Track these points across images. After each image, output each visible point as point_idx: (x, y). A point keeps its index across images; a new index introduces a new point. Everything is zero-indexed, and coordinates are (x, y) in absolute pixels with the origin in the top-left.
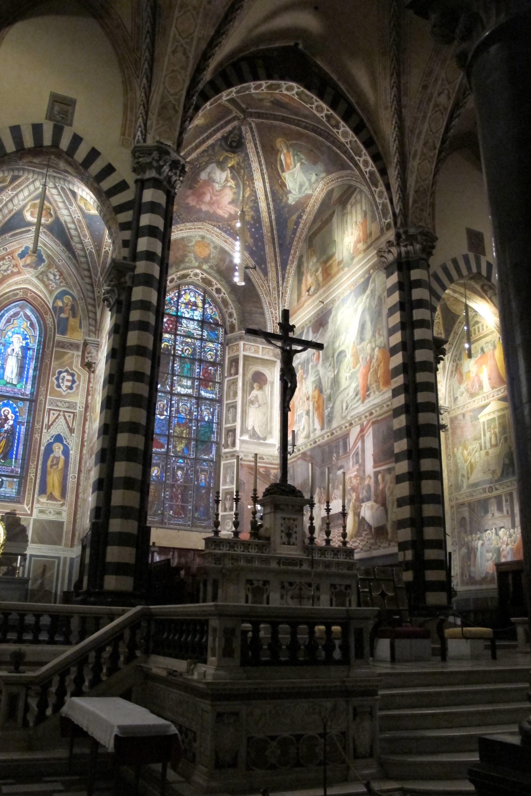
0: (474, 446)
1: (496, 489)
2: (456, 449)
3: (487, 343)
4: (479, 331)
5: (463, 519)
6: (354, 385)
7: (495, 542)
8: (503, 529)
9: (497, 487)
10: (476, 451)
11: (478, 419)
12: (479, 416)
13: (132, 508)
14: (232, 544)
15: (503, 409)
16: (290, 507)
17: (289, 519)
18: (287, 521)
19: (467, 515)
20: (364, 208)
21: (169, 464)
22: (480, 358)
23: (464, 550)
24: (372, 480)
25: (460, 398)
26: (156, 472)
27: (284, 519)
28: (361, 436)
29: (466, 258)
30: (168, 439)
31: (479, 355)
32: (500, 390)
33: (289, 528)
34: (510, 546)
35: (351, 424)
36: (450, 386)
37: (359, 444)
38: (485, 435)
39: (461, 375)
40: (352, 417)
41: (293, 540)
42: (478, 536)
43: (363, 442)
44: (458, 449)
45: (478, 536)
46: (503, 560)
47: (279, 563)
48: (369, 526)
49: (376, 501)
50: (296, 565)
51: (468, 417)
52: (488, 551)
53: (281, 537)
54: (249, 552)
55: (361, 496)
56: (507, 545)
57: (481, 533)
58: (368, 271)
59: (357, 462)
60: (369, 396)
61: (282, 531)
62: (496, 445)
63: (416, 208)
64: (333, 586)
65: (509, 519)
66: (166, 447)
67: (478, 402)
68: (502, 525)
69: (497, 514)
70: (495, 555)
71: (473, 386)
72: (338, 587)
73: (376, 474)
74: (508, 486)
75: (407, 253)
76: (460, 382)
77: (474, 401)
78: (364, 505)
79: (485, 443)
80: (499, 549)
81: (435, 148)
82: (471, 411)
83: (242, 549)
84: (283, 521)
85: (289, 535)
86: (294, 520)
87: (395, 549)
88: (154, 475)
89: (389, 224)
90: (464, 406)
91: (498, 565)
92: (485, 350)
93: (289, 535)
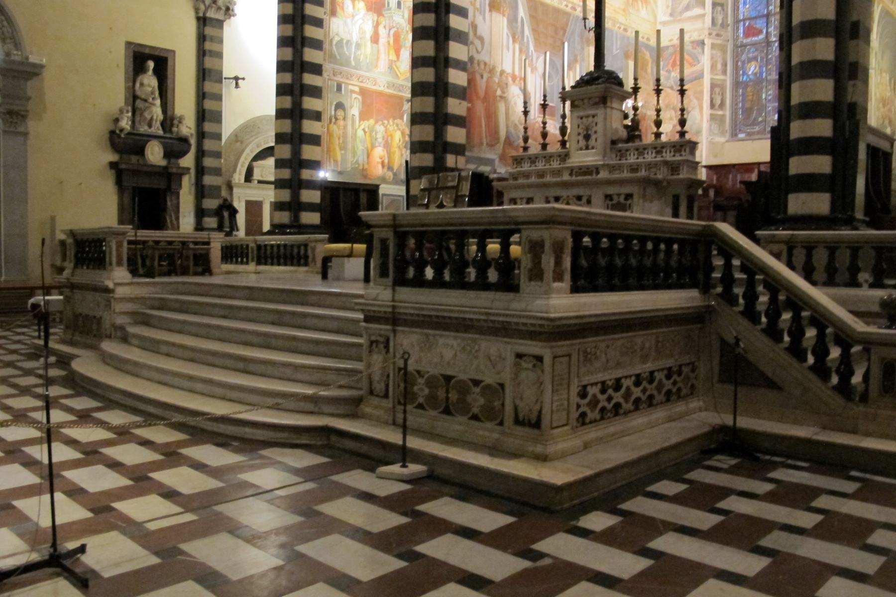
13: (427, 143)
14: (533, 159)
16: (586, 101)
17: (588, 117)
18: (584, 120)
21: (771, 53)
26: (752, 69)
27: (582, 118)
30: (767, 19)
33: (587, 129)
41: (592, 142)
47: (571, 174)
50: (590, 174)
53: (578, 142)
54: (550, 165)
61: (579, 134)
64: (609, 197)
66: (765, 31)
72: (615, 197)
83: (543, 164)
84: (579, 121)
85: (587, 137)
86: (593, 117)
88: (750, 73)
93: (587, 137)
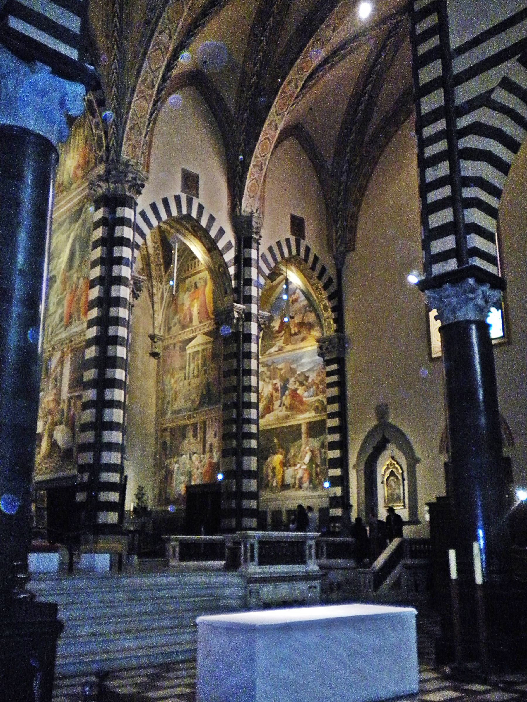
0: (180, 375)
1: (194, 417)
2: (165, 377)
3: (200, 279)
4: (195, 267)
5: (165, 443)
6: (60, 311)
7: (188, 466)
8: (195, 455)
9: (195, 415)
10: (181, 381)
11: (186, 350)
12: (187, 348)
15: (206, 343)
19: (168, 439)
20: (86, 135)
22: (194, 293)
23: (163, 473)
24: (66, 405)
25: (173, 328)
28: (61, 362)
29: (178, 199)
31: (193, 290)
32: (205, 325)
34: (200, 471)
35: (54, 349)
36: (166, 316)
37: (59, 370)
38: (189, 366)
39: (176, 306)
40: (55, 342)
42: (175, 460)
43: (62, 369)
44: (166, 378)
45: (175, 460)
46: (193, 483)
48: (60, 449)
49: (66, 426)
51: (177, 348)
52: (182, 475)
55: (55, 420)
56: (198, 469)
57: (178, 457)
58: (82, 201)
59: (55, 386)
60: (70, 323)
62: (197, 376)
63: (129, 145)
65: (202, 445)
67: (187, 334)
68: (195, 450)
69: (192, 440)
70: (187, 478)
71: (184, 319)
73: (70, 399)
74: (203, 415)
75: (115, 189)
76: (176, 312)
77: (184, 333)
78: (57, 428)
79: (189, 373)
80: (191, 472)
81: (154, 87)
82: (180, 342)
87: (75, 472)
89: (102, 157)
90: (176, 336)
91: (189, 488)
92: (199, 285)
